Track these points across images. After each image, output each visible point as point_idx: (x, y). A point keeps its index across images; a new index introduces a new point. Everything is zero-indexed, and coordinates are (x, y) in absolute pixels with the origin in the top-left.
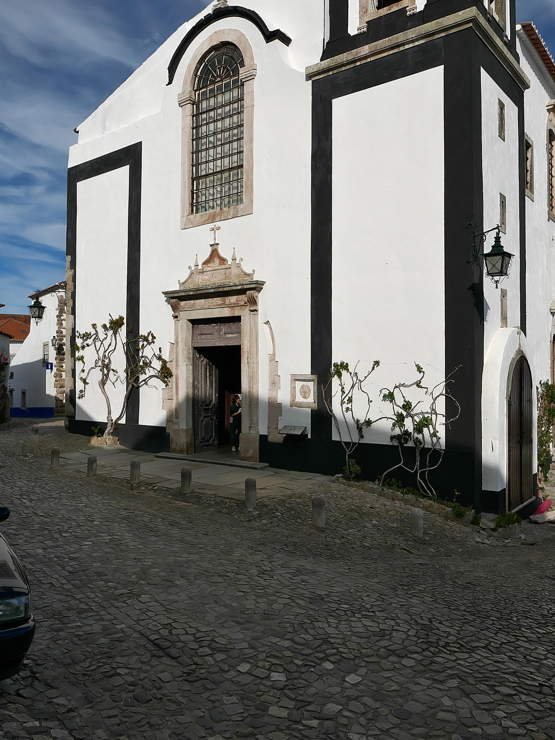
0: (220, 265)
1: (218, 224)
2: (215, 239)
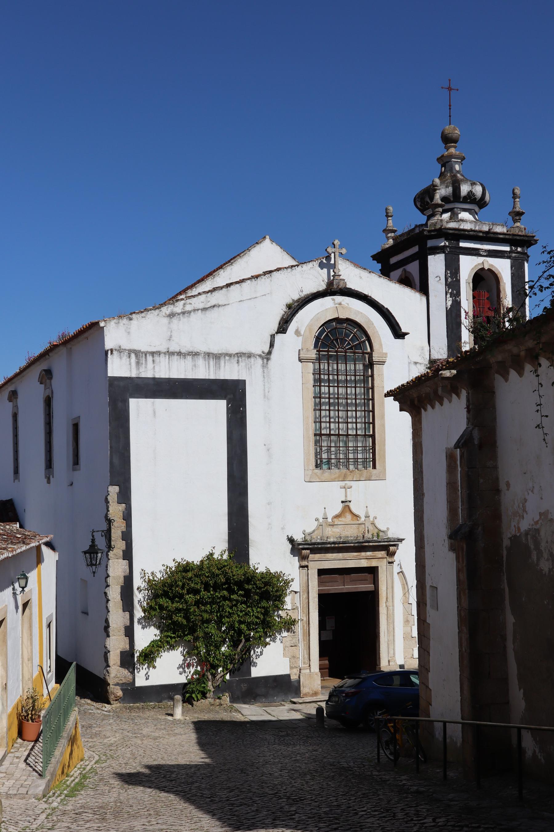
1: (349, 483)
2: (346, 496)
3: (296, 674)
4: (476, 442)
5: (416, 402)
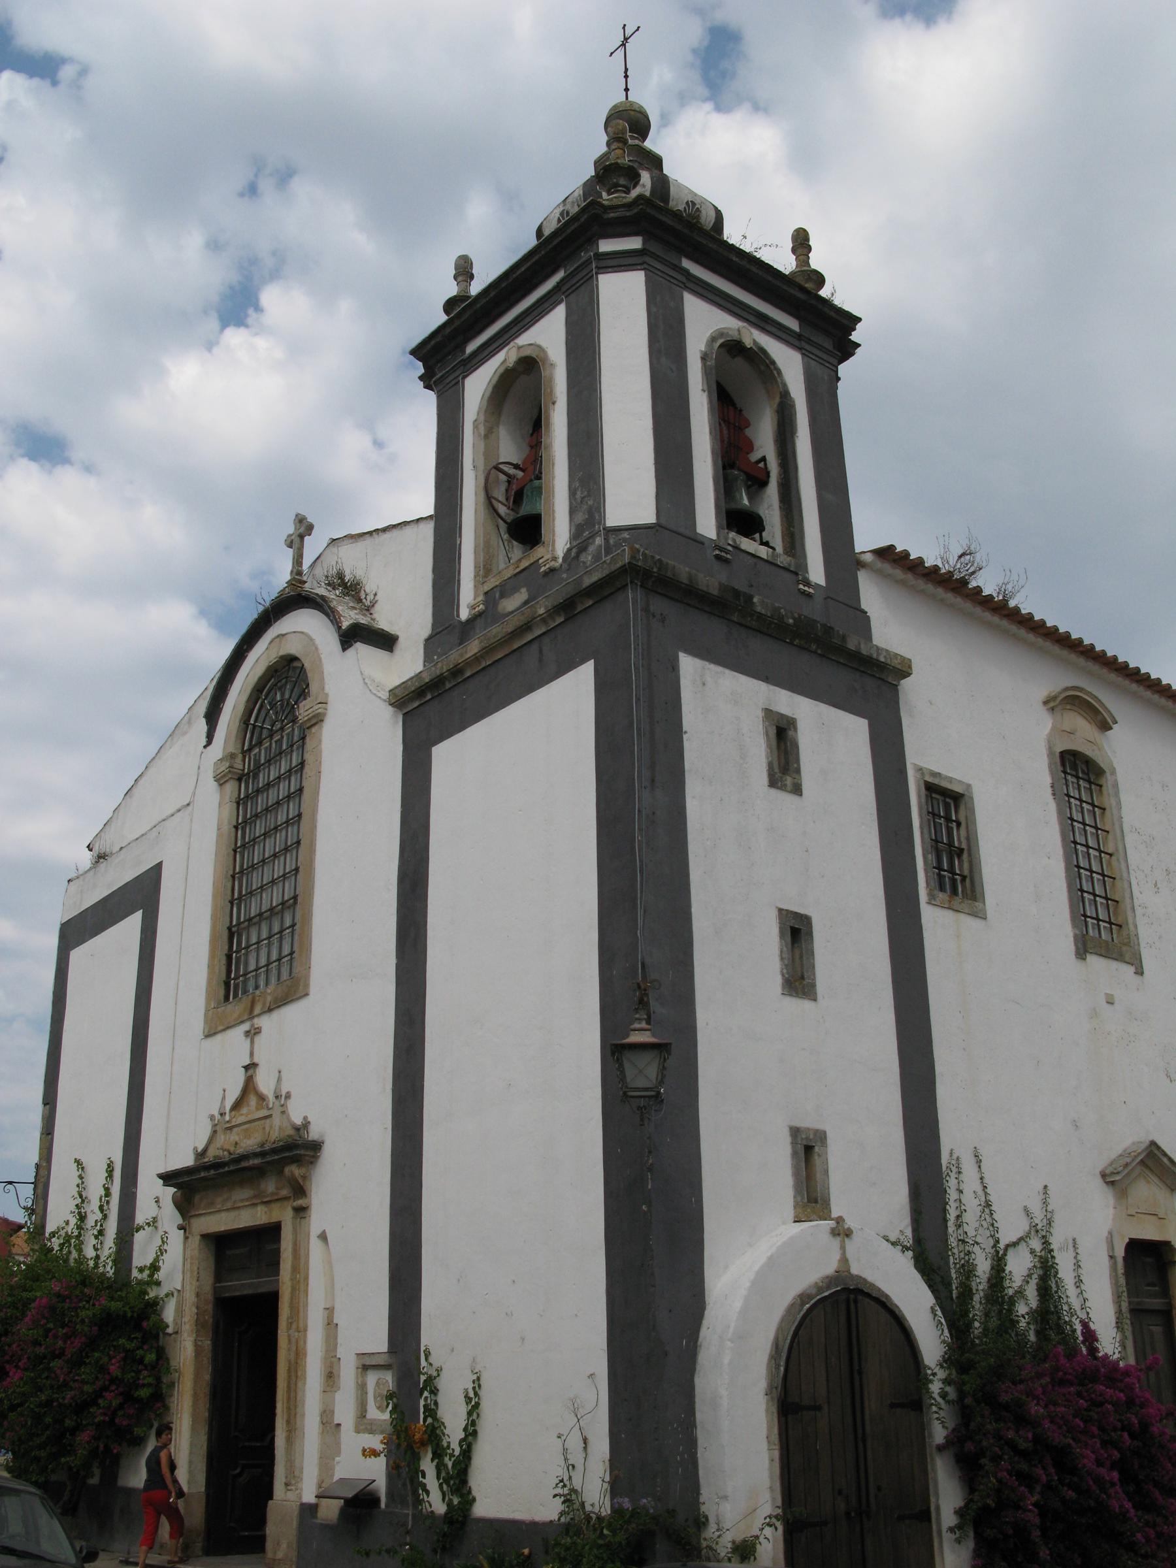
0: (257, 1109)
2: (252, 1054)
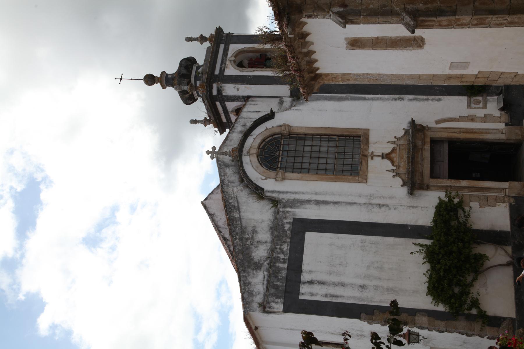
0: (396, 153)
2: (379, 156)
3: (509, 199)
4: (342, 9)
5: (312, 75)
